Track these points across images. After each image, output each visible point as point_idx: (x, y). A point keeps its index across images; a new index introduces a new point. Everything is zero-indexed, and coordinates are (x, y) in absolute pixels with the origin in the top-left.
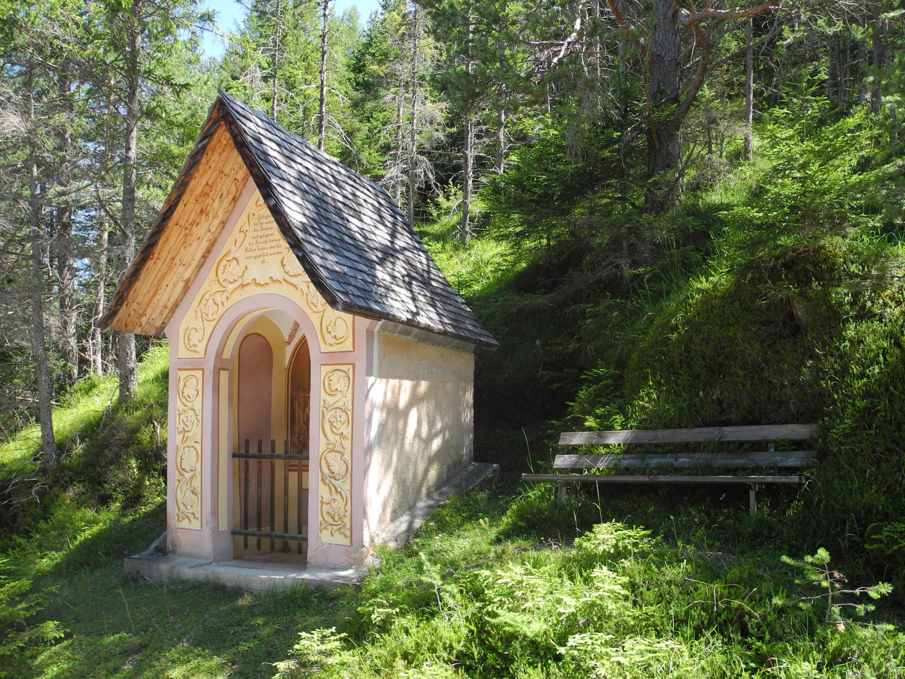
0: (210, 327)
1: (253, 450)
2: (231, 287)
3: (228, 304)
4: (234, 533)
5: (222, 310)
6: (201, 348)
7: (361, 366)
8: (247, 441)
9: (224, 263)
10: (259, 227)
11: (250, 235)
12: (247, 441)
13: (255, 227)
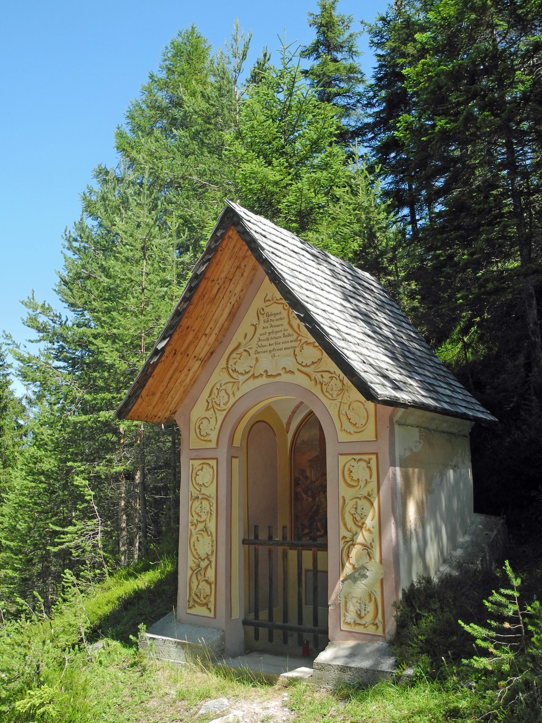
0: (221, 416)
1: (263, 536)
2: (242, 378)
3: (238, 395)
4: (245, 623)
5: (232, 400)
6: (214, 436)
7: (385, 456)
8: (256, 527)
9: (234, 355)
10: (267, 324)
11: (260, 331)
12: (256, 527)
13: (266, 325)
